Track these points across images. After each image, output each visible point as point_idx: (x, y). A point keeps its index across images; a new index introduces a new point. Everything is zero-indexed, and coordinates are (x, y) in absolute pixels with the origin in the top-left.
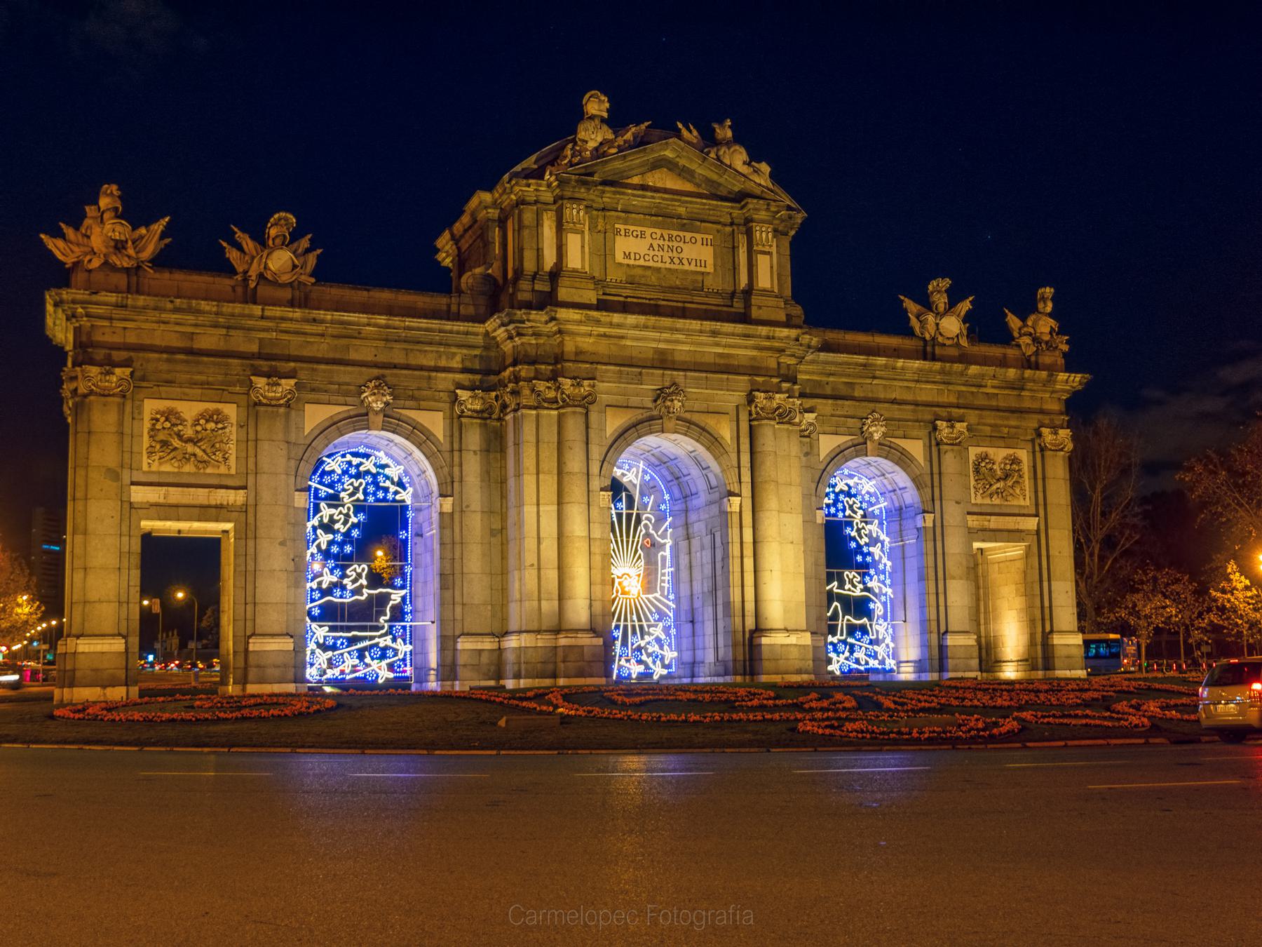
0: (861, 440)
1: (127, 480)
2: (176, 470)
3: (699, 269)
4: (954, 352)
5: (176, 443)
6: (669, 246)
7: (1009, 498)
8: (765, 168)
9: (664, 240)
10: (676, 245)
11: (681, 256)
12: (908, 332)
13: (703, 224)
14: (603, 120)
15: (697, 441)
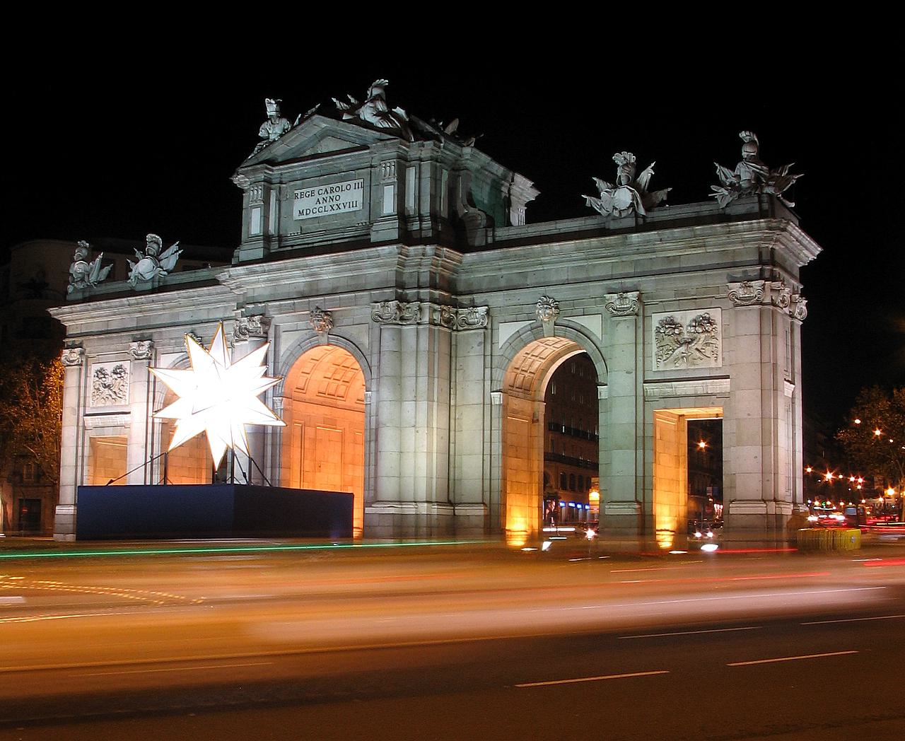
0: (539, 324)
1: (81, 414)
2: (103, 405)
3: (352, 209)
4: (630, 222)
5: (102, 389)
6: (330, 197)
7: (699, 361)
8: (399, 111)
9: (327, 193)
10: (335, 194)
11: (338, 203)
12: (592, 212)
13: (357, 171)
14: (280, 117)
15: (345, 349)
